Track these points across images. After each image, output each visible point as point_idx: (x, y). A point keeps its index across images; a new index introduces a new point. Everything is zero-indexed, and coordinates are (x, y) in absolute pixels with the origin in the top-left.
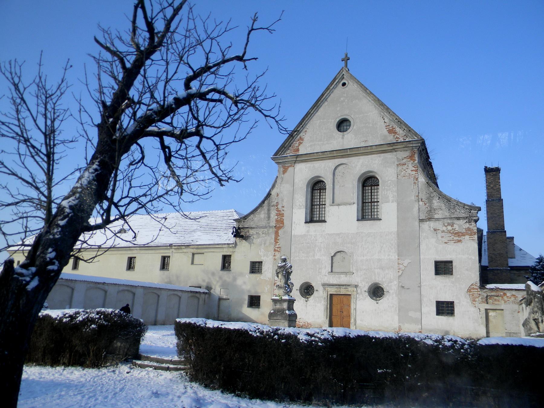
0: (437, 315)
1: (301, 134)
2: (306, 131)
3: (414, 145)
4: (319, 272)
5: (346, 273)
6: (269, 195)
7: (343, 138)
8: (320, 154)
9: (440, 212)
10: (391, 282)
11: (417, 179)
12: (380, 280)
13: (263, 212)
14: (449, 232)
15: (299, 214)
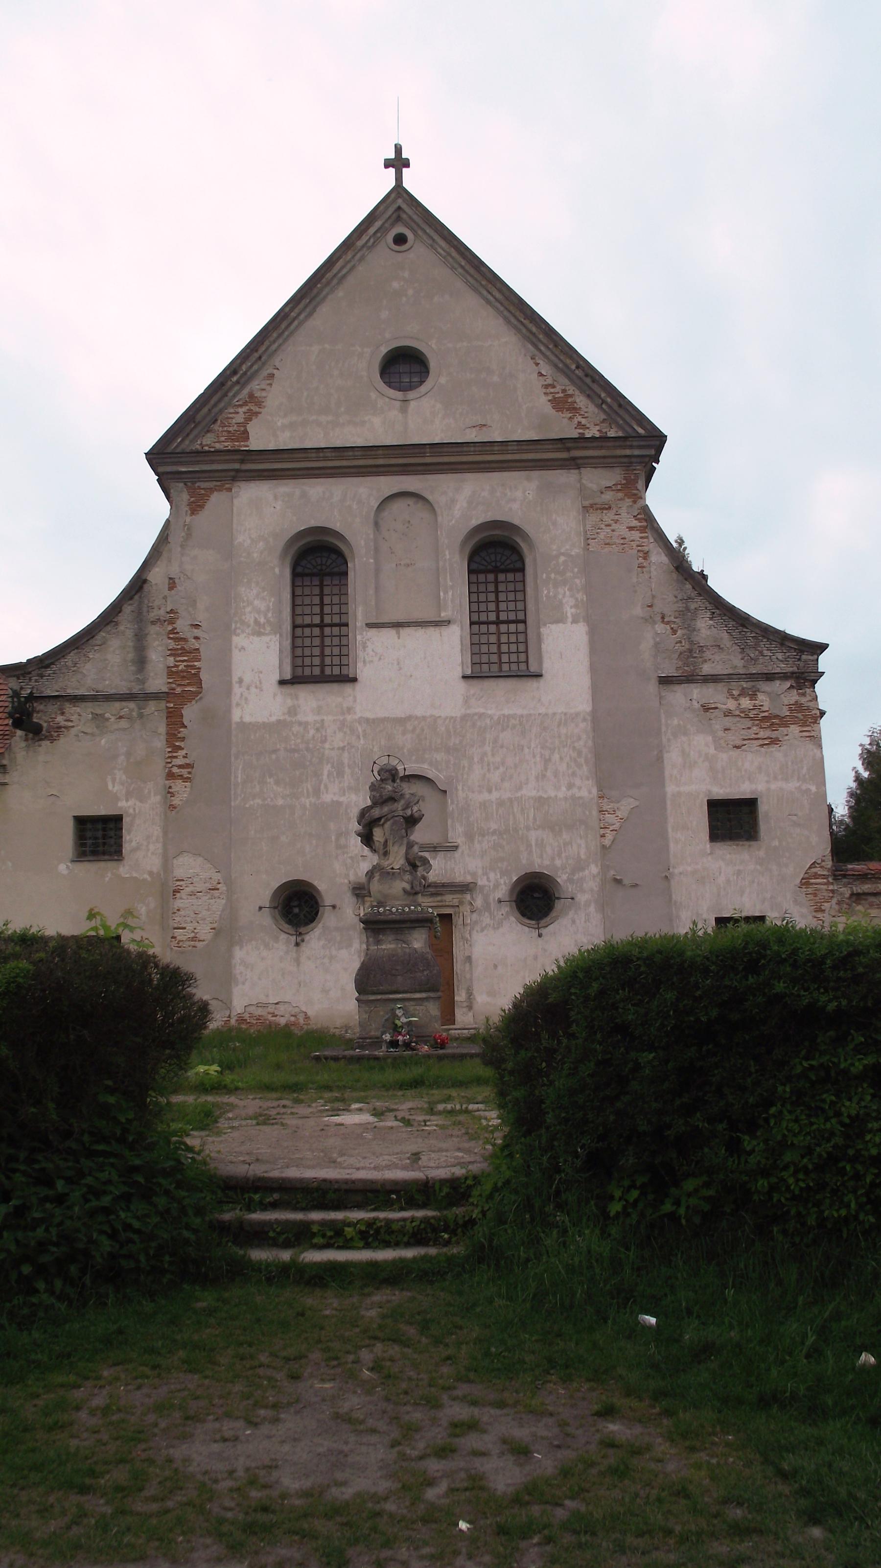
1: (255, 386)
2: (272, 376)
3: (637, 452)
4: (339, 847)
6: (137, 586)
7: (404, 411)
10: (582, 869)
11: (646, 555)
12: (547, 862)
13: (115, 643)
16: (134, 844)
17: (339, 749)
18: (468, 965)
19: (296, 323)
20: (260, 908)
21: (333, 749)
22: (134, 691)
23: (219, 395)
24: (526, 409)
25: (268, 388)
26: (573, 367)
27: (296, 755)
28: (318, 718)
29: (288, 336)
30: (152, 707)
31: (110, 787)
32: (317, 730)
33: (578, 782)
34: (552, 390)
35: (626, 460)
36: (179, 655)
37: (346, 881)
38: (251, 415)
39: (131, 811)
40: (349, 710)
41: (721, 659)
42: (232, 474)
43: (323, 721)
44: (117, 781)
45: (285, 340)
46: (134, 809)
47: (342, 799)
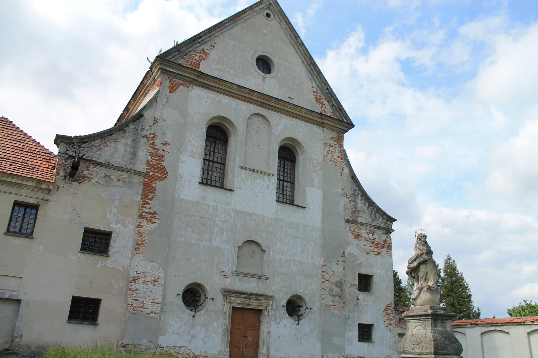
0: (359, 341)
1: (206, 47)
5: (259, 277)
8: (235, 87)
9: (363, 216)
12: (302, 291)
13: (122, 141)
14: (370, 241)
15: (189, 165)
16: (116, 249)
19: (226, 29)
20: (178, 295)
22: (128, 168)
23: (191, 44)
24: (306, 98)
25: (211, 50)
28: (215, 204)
30: (136, 178)
31: (108, 216)
32: (214, 210)
33: (315, 257)
35: (339, 130)
36: (155, 157)
37: (219, 287)
39: (118, 231)
40: (229, 204)
42: (192, 80)
44: (112, 213)
45: (221, 34)
46: (119, 231)
47: (221, 246)
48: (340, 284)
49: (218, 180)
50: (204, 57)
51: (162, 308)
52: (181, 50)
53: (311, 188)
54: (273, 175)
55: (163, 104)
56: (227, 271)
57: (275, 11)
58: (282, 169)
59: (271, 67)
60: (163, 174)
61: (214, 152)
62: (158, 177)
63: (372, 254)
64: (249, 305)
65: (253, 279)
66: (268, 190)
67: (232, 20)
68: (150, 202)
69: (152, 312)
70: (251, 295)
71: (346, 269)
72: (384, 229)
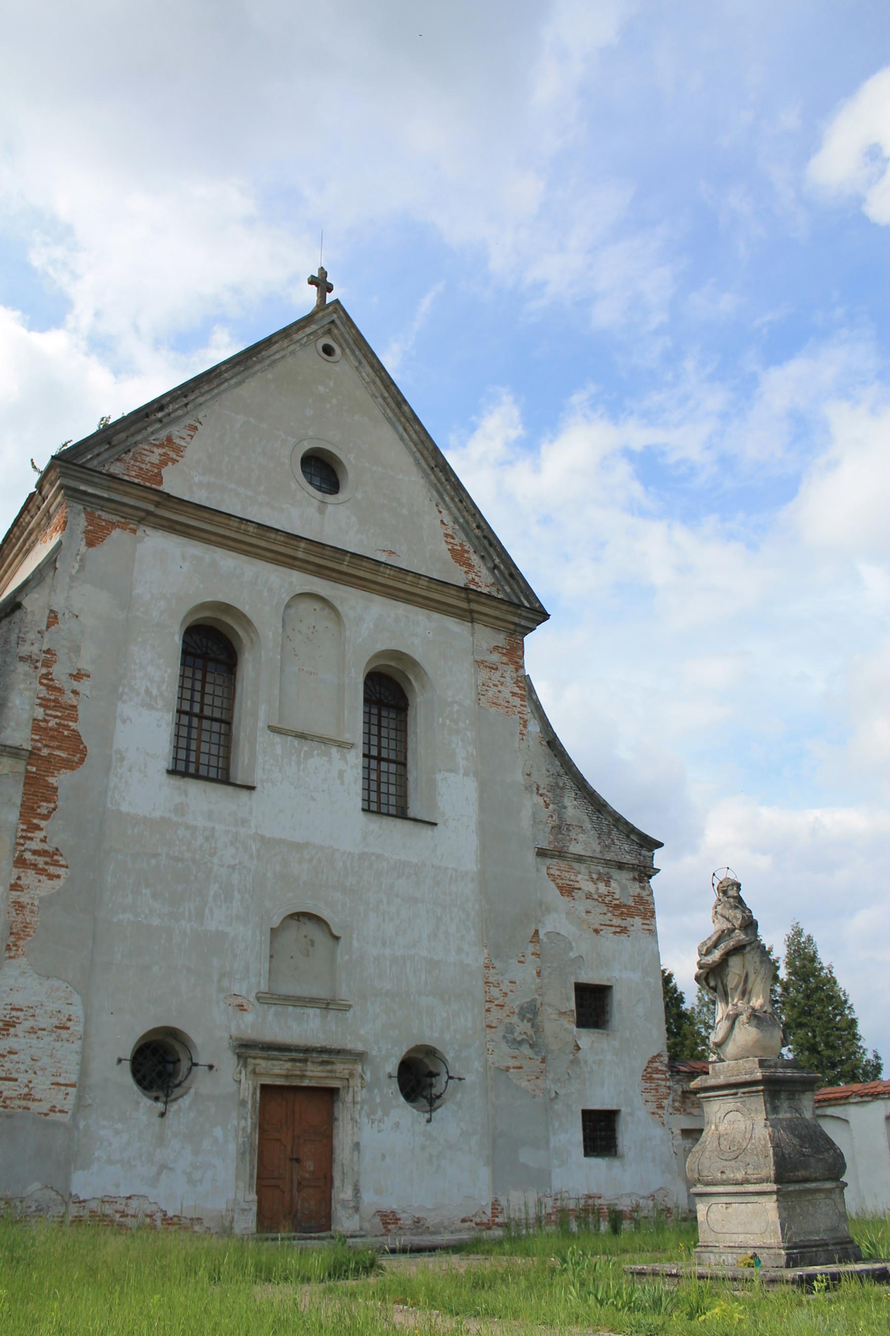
0: (587, 1154)
1: (176, 431)
5: (327, 1005)
7: (321, 511)
8: (251, 529)
9: (582, 837)
12: (436, 1035)
14: (601, 899)
15: (141, 727)
17: (229, 866)
18: (356, 1153)
19: (226, 385)
20: (120, 1061)
21: (223, 866)
23: (140, 425)
24: (429, 551)
25: (188, 439)
26: (474, 525)
27: (180, 865)
29: (216, 395)
32: (207, 839)
34: (452, 541)
35: (512, 627)
36: (54, 708)
37: (227, 1036)
38: (165, 461)
40: (244, 822)
41: (584, 841)
42: (142, 514)
43: (213, 829)
45: (212, 398)
48: (530, 1012)
49: (214, 762)
50: (173, 455)
51: (80, 1098)
52: (115, 440)
53: (447, 774)
54: (352, 745)
55: (72, 577)
56: (244, 993)
57: (346, 341)
58: (374, 730)
59: (340, 477)
60: (75, 750)
61: (203, 693)
62: (63, 759)
63: (607, 932)
64: (303, 1077)
65: (311, 1012)
66: (342, 783)
67: (239, 363)
68: (43, 824)
69: (53, 1109)
70: (307, 1051)
71: (545, 973)
72: (633, 868)
